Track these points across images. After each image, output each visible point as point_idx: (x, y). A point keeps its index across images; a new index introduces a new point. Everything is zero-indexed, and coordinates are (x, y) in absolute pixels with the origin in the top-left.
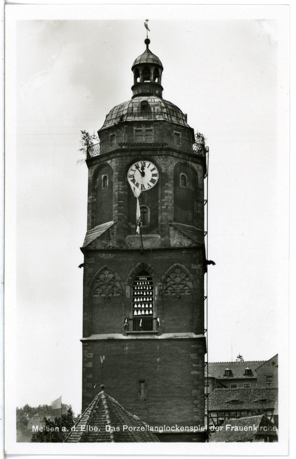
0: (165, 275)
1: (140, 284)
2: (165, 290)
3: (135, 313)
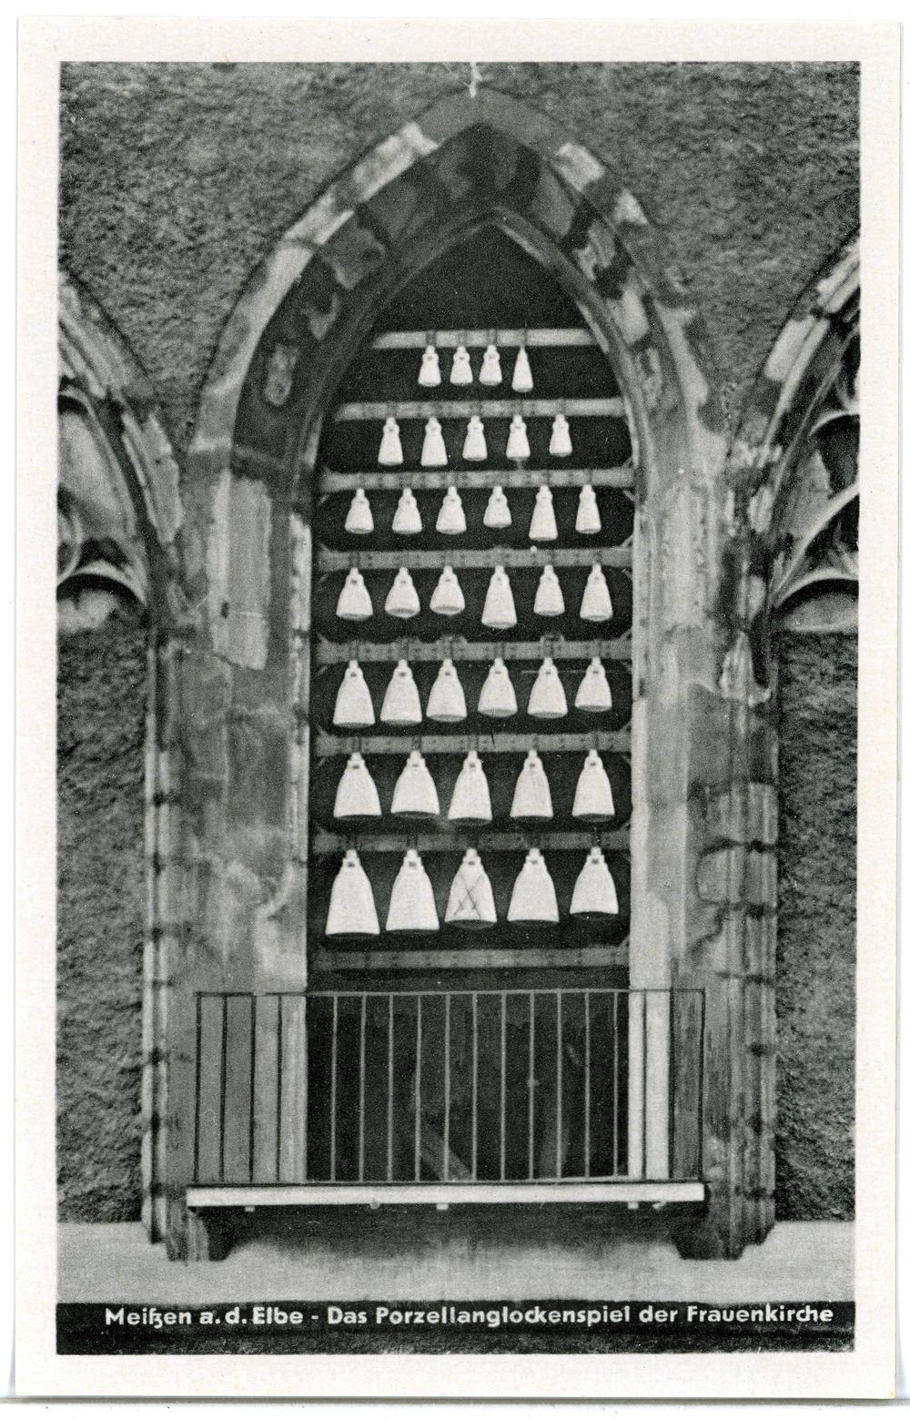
0: (818, 313)
1: (434, 450)
2: (819, 551)
3: (352, 907)
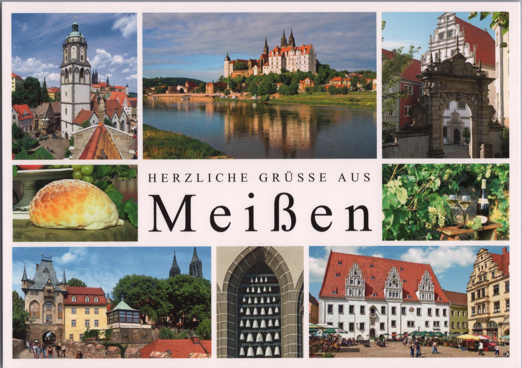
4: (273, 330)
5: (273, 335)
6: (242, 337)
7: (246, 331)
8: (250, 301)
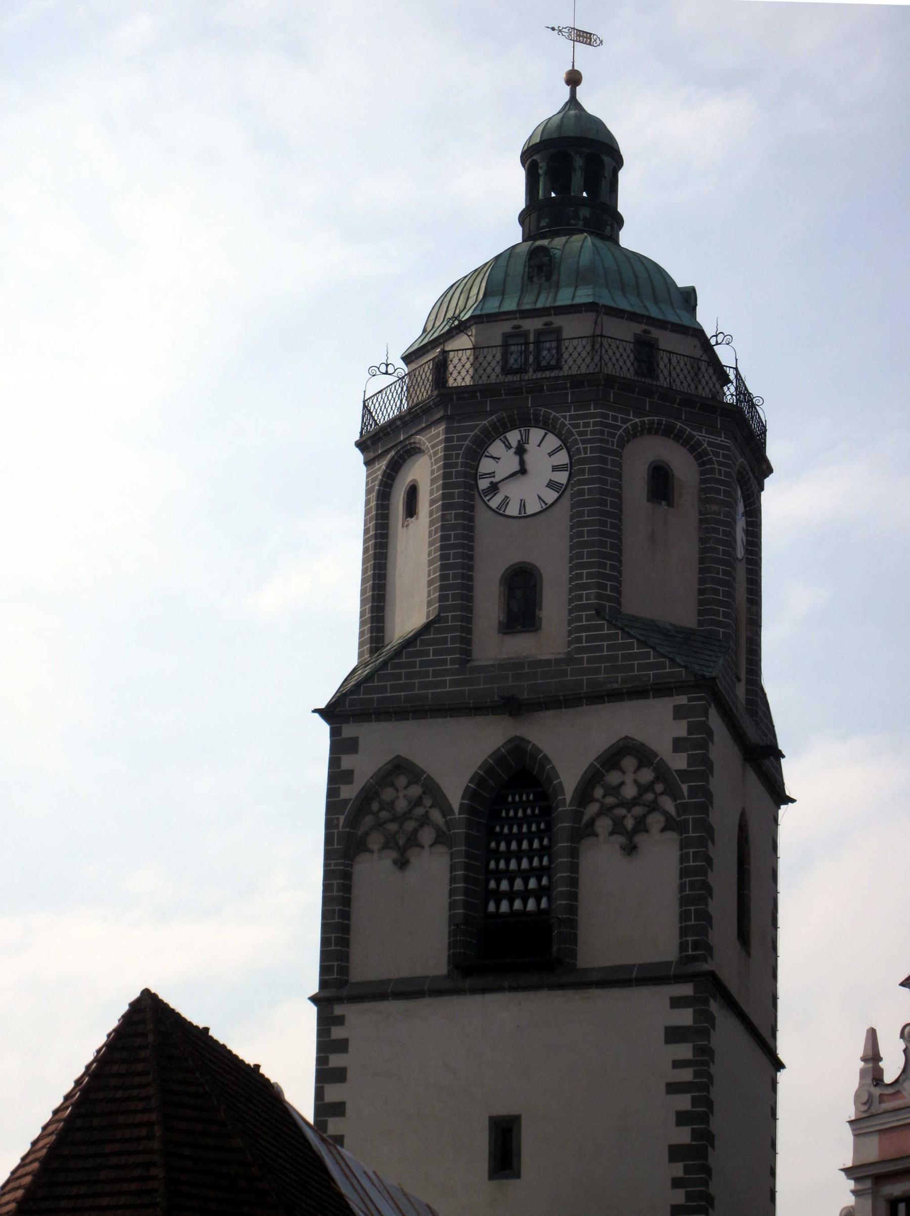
3: (492, 907)
4: (539, 872)
5: (539, 880)
6: (492, 884)
7: (499, 875)
8: (506, 830)
